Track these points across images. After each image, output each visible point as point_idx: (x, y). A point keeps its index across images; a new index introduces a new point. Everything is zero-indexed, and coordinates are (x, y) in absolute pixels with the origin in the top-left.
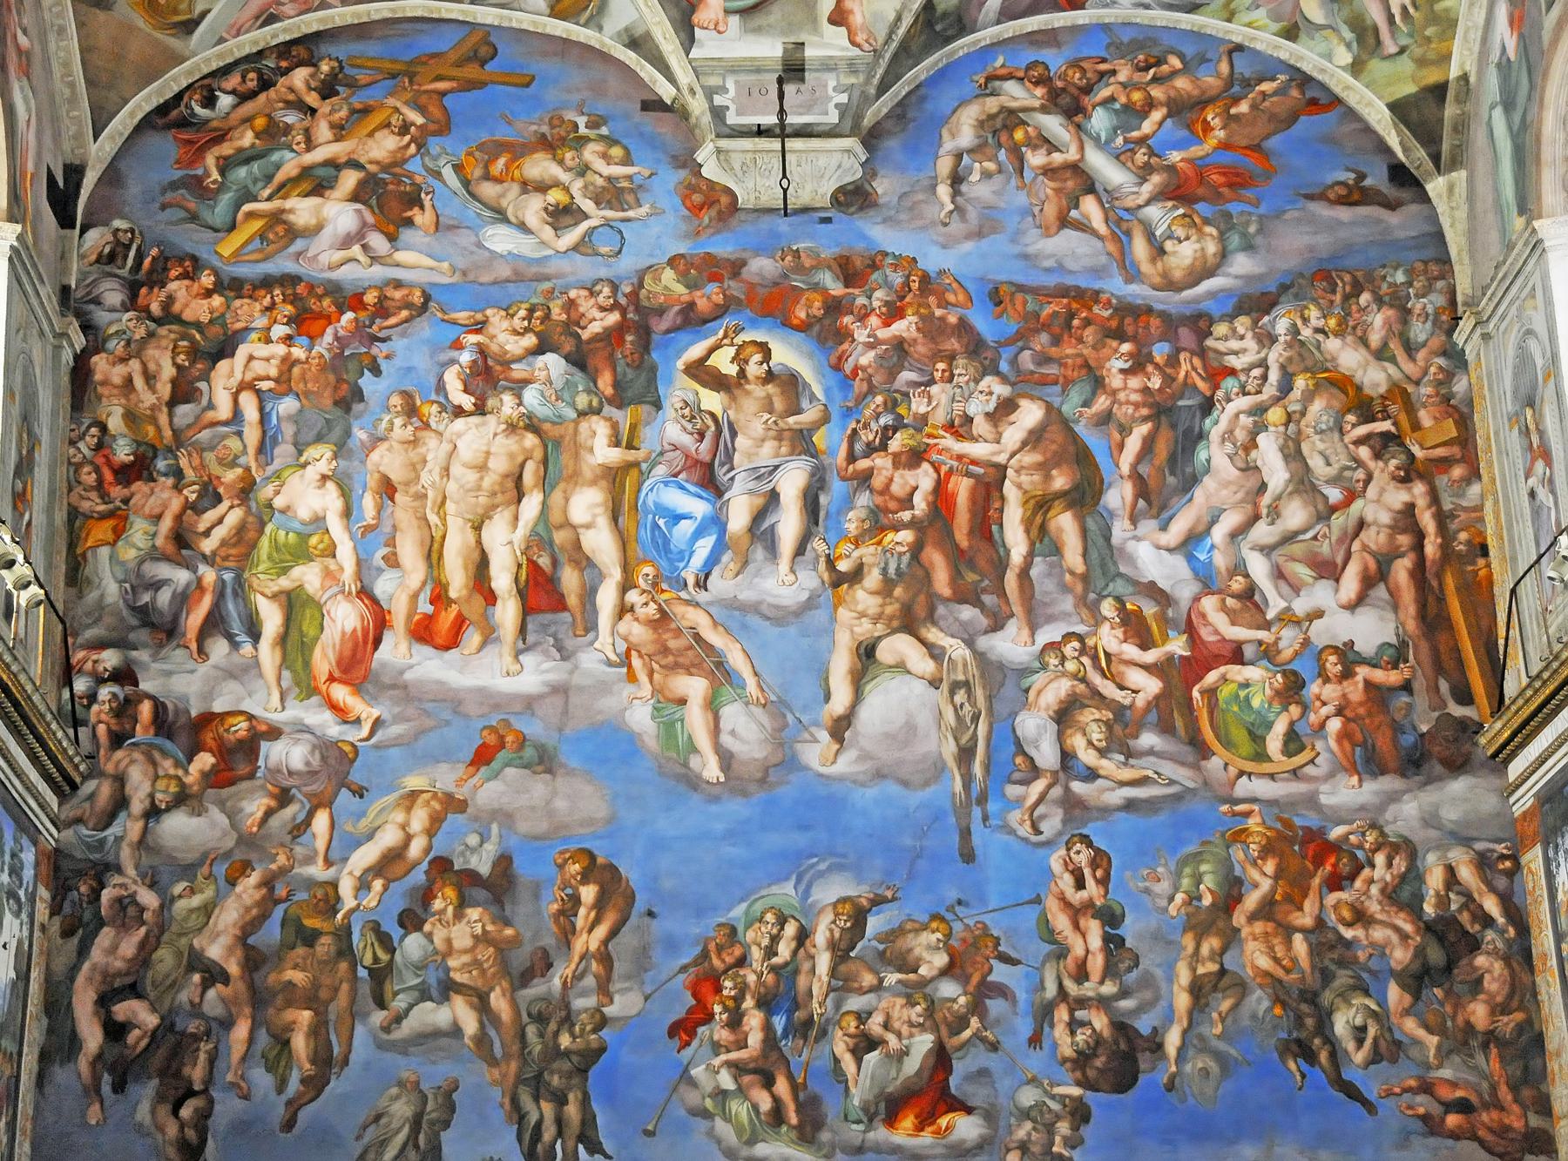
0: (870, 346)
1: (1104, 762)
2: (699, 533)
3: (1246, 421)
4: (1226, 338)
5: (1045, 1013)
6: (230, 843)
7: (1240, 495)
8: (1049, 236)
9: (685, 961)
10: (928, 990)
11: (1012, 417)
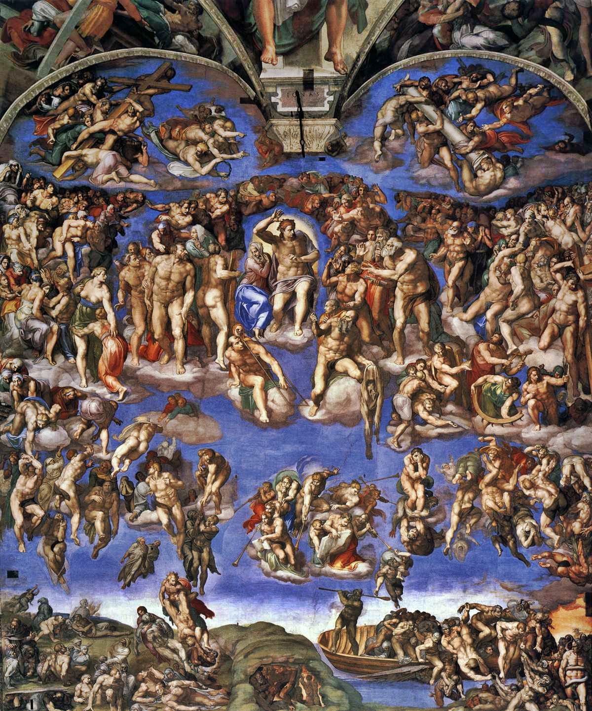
0: (340, 222)
1: (431, 417)
2: (261, 311)
3: (507, 260)
4: (501, 220)
5: (397, 523)
6: (68, 442)
7: (500, 296)
8: (423, 167)
9: (251, 496)
10: (350, 512)
11: (402, 258)
